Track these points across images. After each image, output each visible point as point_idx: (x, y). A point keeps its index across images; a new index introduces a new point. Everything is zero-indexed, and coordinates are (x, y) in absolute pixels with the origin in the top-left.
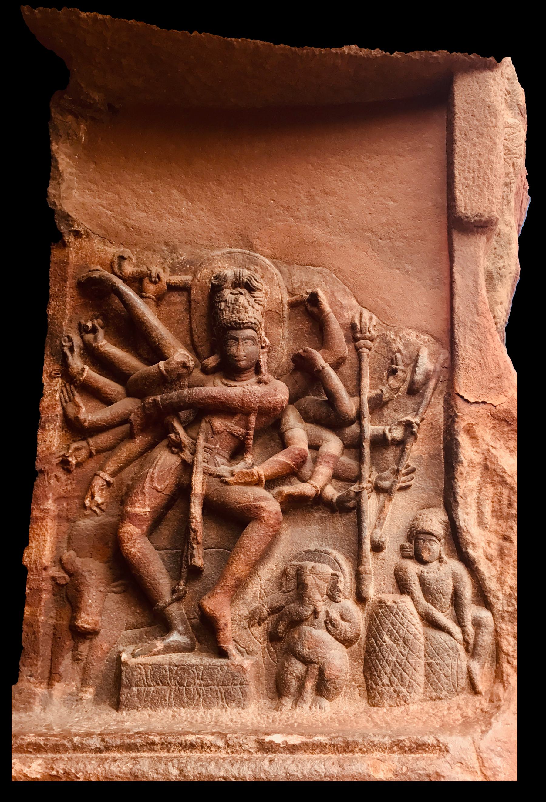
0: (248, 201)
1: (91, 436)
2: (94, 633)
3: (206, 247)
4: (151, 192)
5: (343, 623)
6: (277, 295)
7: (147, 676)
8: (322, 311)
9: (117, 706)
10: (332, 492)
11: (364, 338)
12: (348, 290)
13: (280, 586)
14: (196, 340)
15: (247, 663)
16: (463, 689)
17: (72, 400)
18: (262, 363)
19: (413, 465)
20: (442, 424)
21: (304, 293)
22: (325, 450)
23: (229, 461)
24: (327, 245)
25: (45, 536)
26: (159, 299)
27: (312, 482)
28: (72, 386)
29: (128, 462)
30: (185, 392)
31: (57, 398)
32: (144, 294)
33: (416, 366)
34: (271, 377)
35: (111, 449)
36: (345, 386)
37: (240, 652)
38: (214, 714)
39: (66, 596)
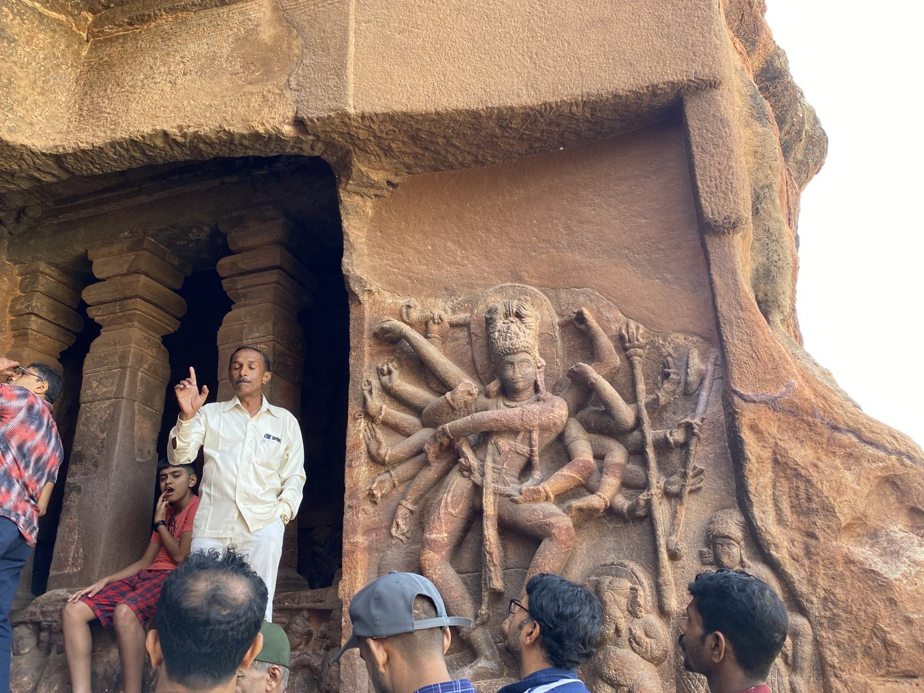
0: (514, 242)
1: (394, 468)
3: (480, 285)
5: (648, 640)
8: (589, 328)
17: (375, 437)
18: (539, 383)
19: (701, 466)
21: (571, 312)
23: (519, 479)
24: (589, 268)
27: (599, 493)
31: (361, 436)
34: (549, 395)
35: (412, 478)
36: (621, 394)
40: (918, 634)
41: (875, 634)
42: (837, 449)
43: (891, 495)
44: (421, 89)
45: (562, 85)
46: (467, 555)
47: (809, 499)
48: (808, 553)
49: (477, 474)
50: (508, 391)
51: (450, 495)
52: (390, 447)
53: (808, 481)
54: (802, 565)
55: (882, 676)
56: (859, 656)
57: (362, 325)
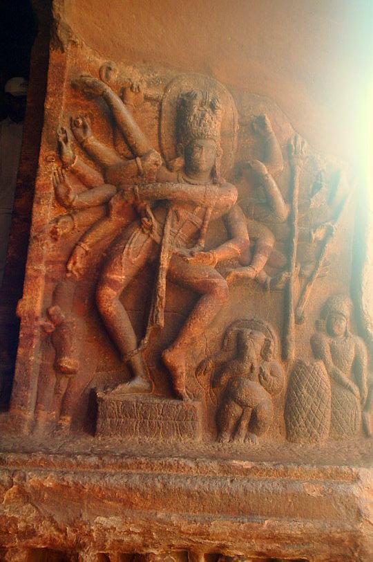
1: (75, 213)
2: (74, 372)
4: (134, 17)
5: (272, 378)
7: (118, 409)
8: (267, 134)
14: (164, 143)
15: (197, 404)
17: (63, 182)
22: (263, 242)
25: (37, 291)
28: (63, 171)
31: (51, 179)
35: (91, 227)
49: (156, 233)
51: (132, 246)
52: (77, 196)
57: (63, 74)
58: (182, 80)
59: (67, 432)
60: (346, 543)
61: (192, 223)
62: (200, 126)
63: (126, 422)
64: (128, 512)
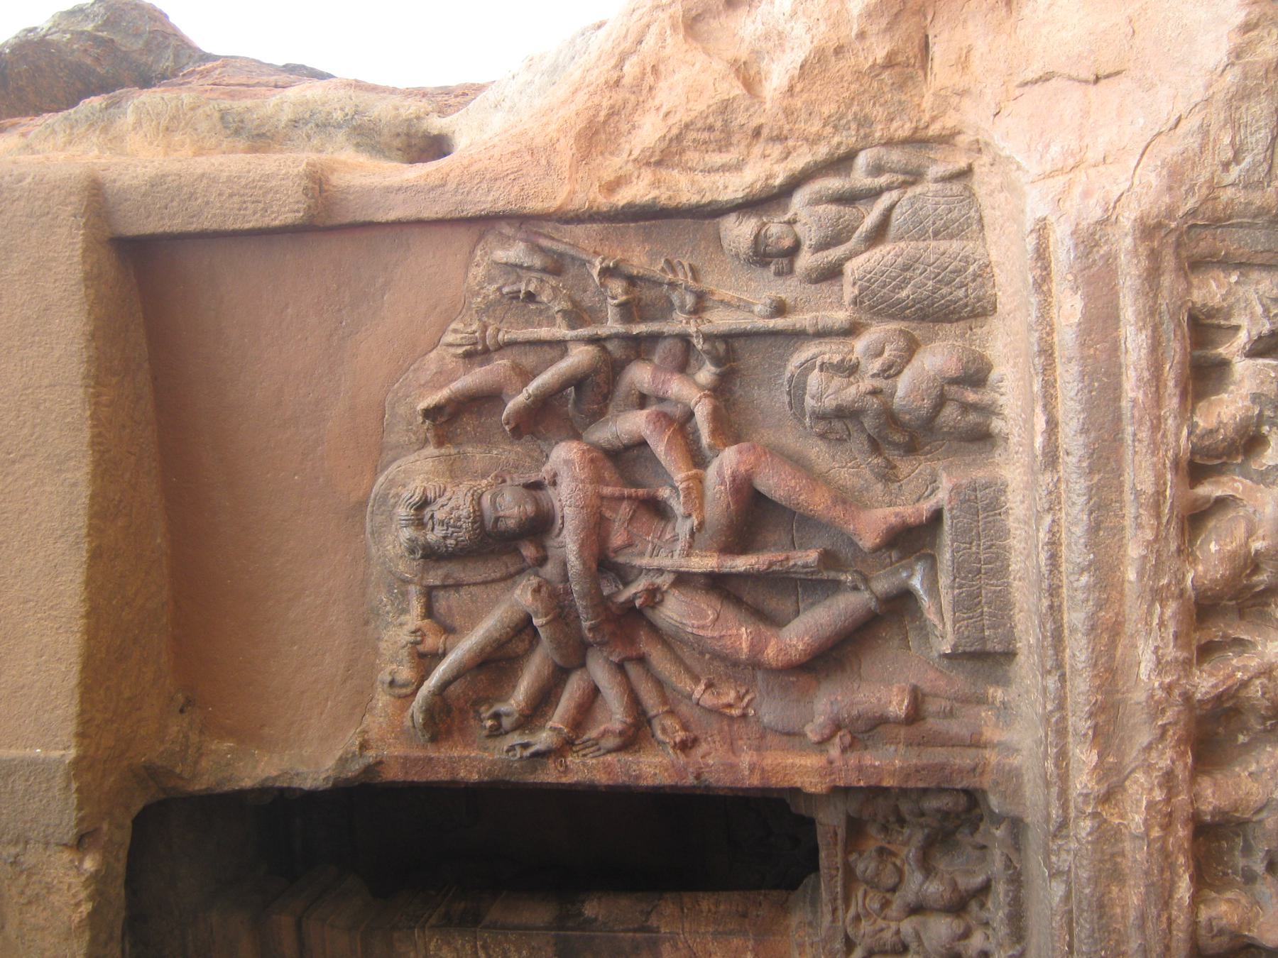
1: (644, 713)
5: (886, 354)
6: (429, 465)
8: (449, 401)
9: (1010, 655)
10: (706, 374)
11: (484, 339)
12: (416, 365)
13: (841, 440)
14: (498, 575)
15: (945, 483)
16: (966, 187)
17: (596, 742)
20: (601, 226)
26: (448, 630)
27: (693, 403)
29: (679, 660)
30: (576, 588)
31: (594, 761)
32: (440, 651)
33: (521, 267)
34: (548, 467)
35: (660, 684)
36: (552, 362)
37: (933, 491)
38: (1016, 525)
39: (866, 732)
40: (875, 28)
41: (877, 75)
42: (645, 86)
43: (708, 24)
44: (45, 640)
45: (65, 416)
46: (773, 604)
47: (711, 128)
48: (780, 138)
50: (540, 526)
52: (614, 714)
53: (687, 126)
54: (795, 148)
55: (926, 75)
56: (903, 98)
57: (417, 760)
58: (385, 555)
59: (1013, 690)
60: (1156, 244)
61: (631, 518)
62: (460, 527)
63: (989, 603)
64: (1129, 628)
